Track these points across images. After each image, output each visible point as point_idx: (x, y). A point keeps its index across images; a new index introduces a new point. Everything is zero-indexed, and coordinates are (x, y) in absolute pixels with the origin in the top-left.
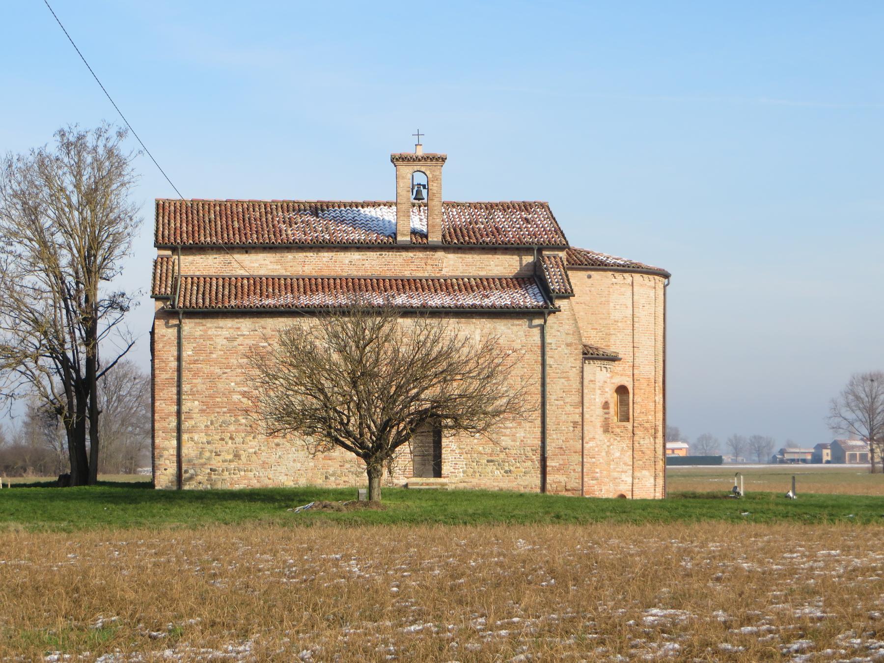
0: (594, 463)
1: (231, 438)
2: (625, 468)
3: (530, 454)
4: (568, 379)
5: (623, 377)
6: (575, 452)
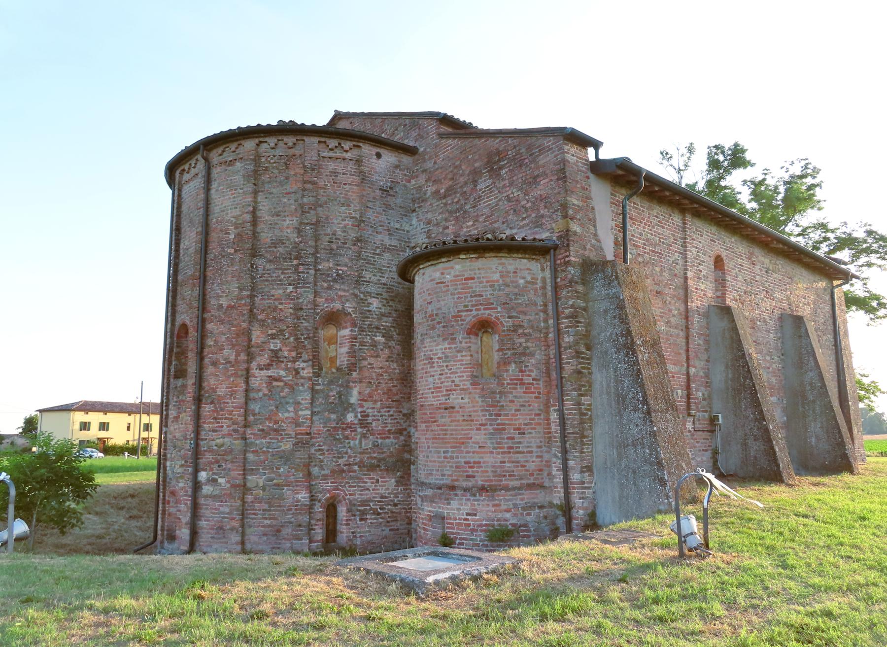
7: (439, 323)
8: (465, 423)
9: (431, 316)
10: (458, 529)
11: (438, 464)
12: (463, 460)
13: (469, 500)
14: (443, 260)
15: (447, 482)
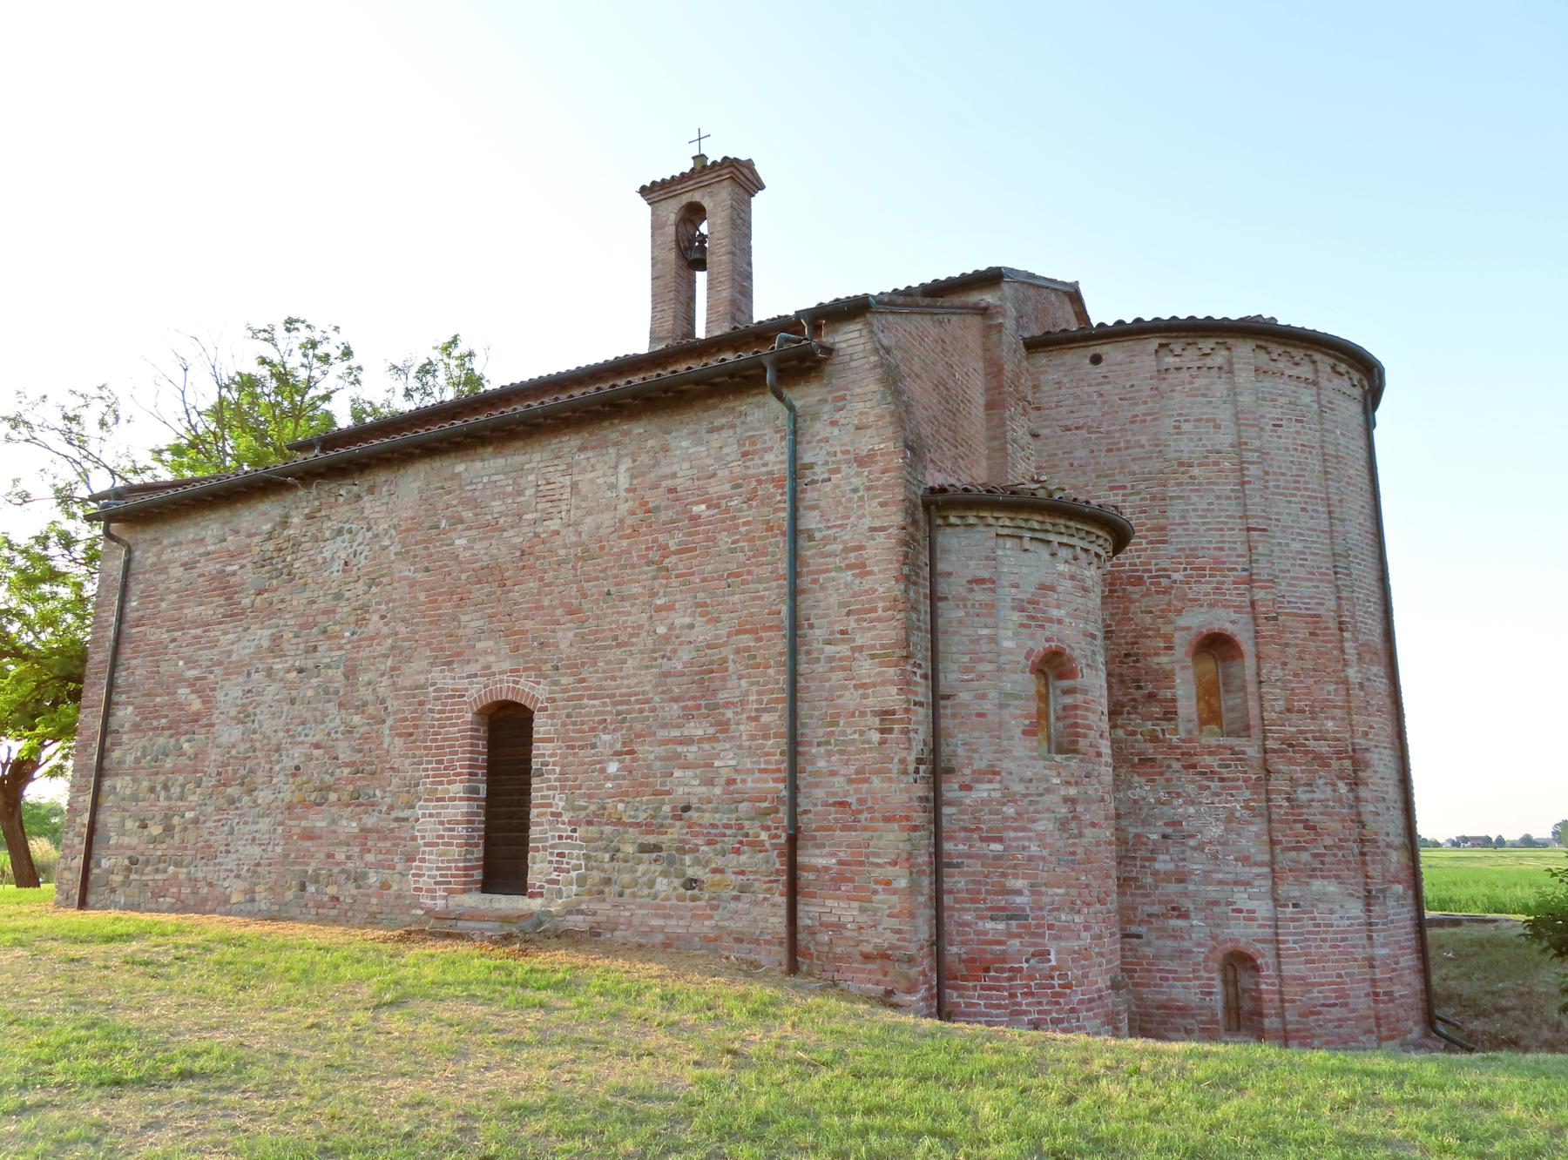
0: (997, 858)
1: (166, 787)
2: (1245, 872)
3: (752, 828)
4: (861, 569)
5: (1220, 612)
6: (887, 820)
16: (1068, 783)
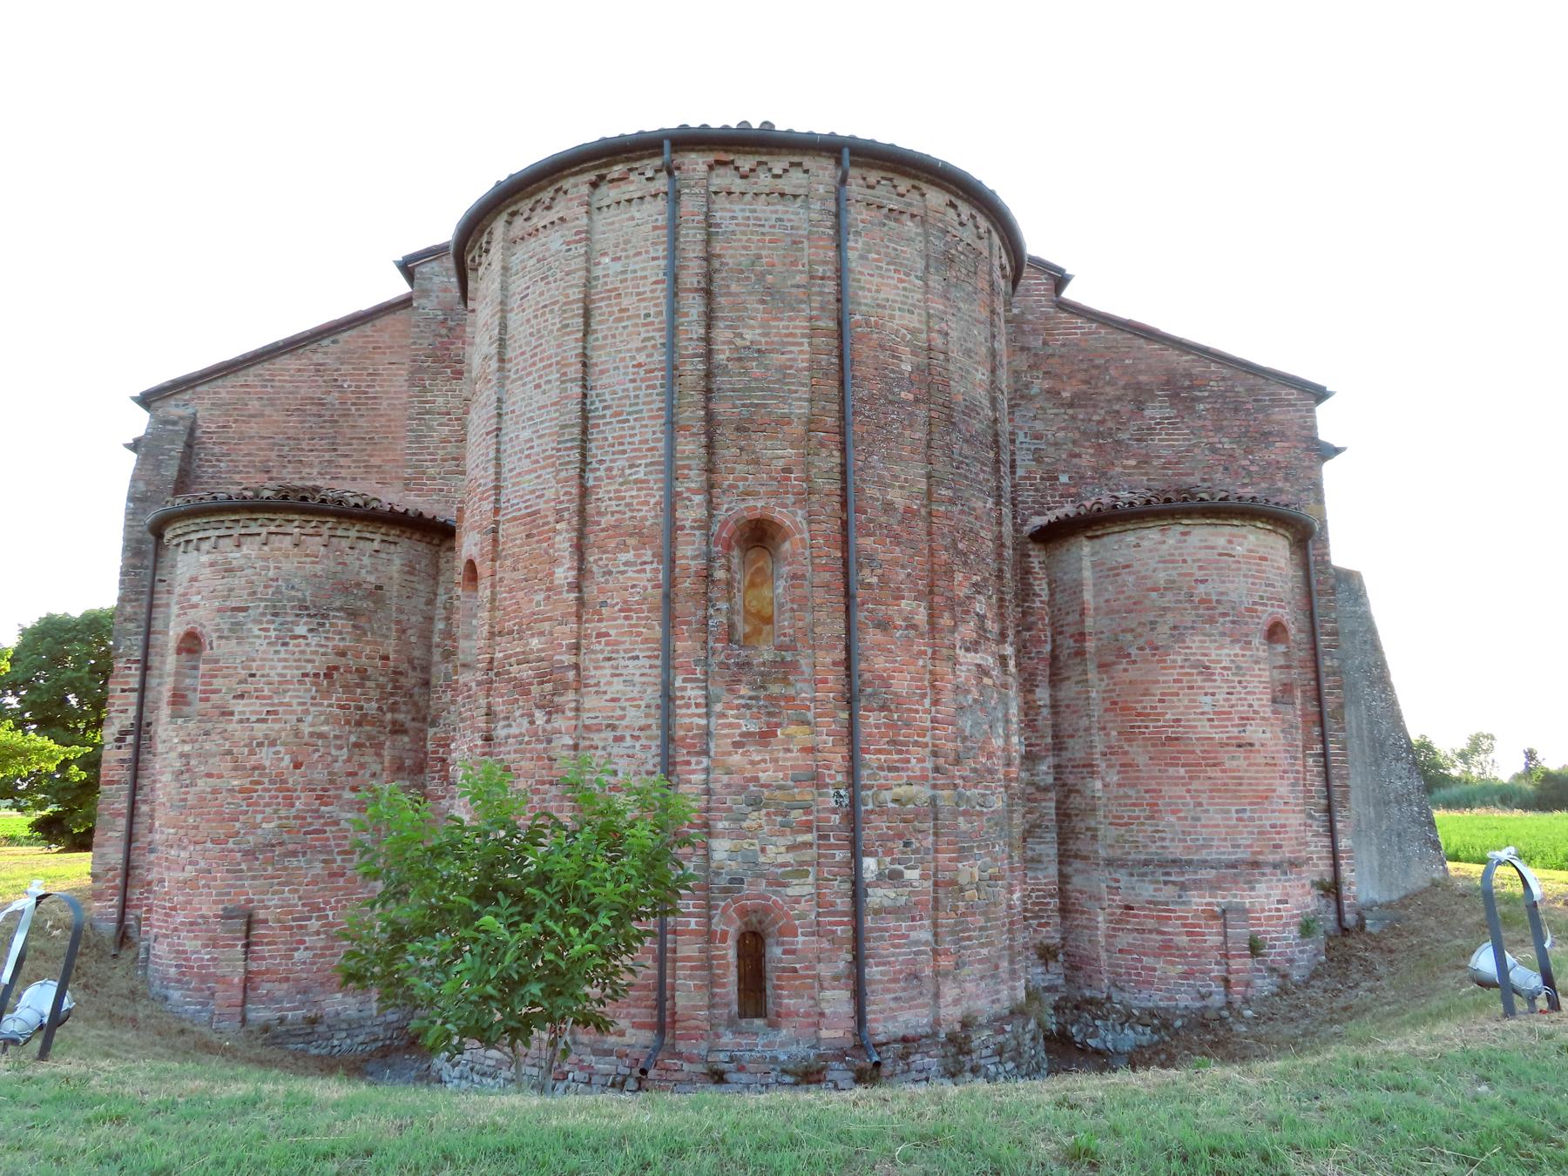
7: (1224, 615)
8: (1268, 768)
9: (1202, 601)
10: (1267, 925)
11: (1224, 830)
12: (1268, 823)
13: (1279, 880)
14: (1235, 522)
15: (1244, 856)
16: (184, 742)
